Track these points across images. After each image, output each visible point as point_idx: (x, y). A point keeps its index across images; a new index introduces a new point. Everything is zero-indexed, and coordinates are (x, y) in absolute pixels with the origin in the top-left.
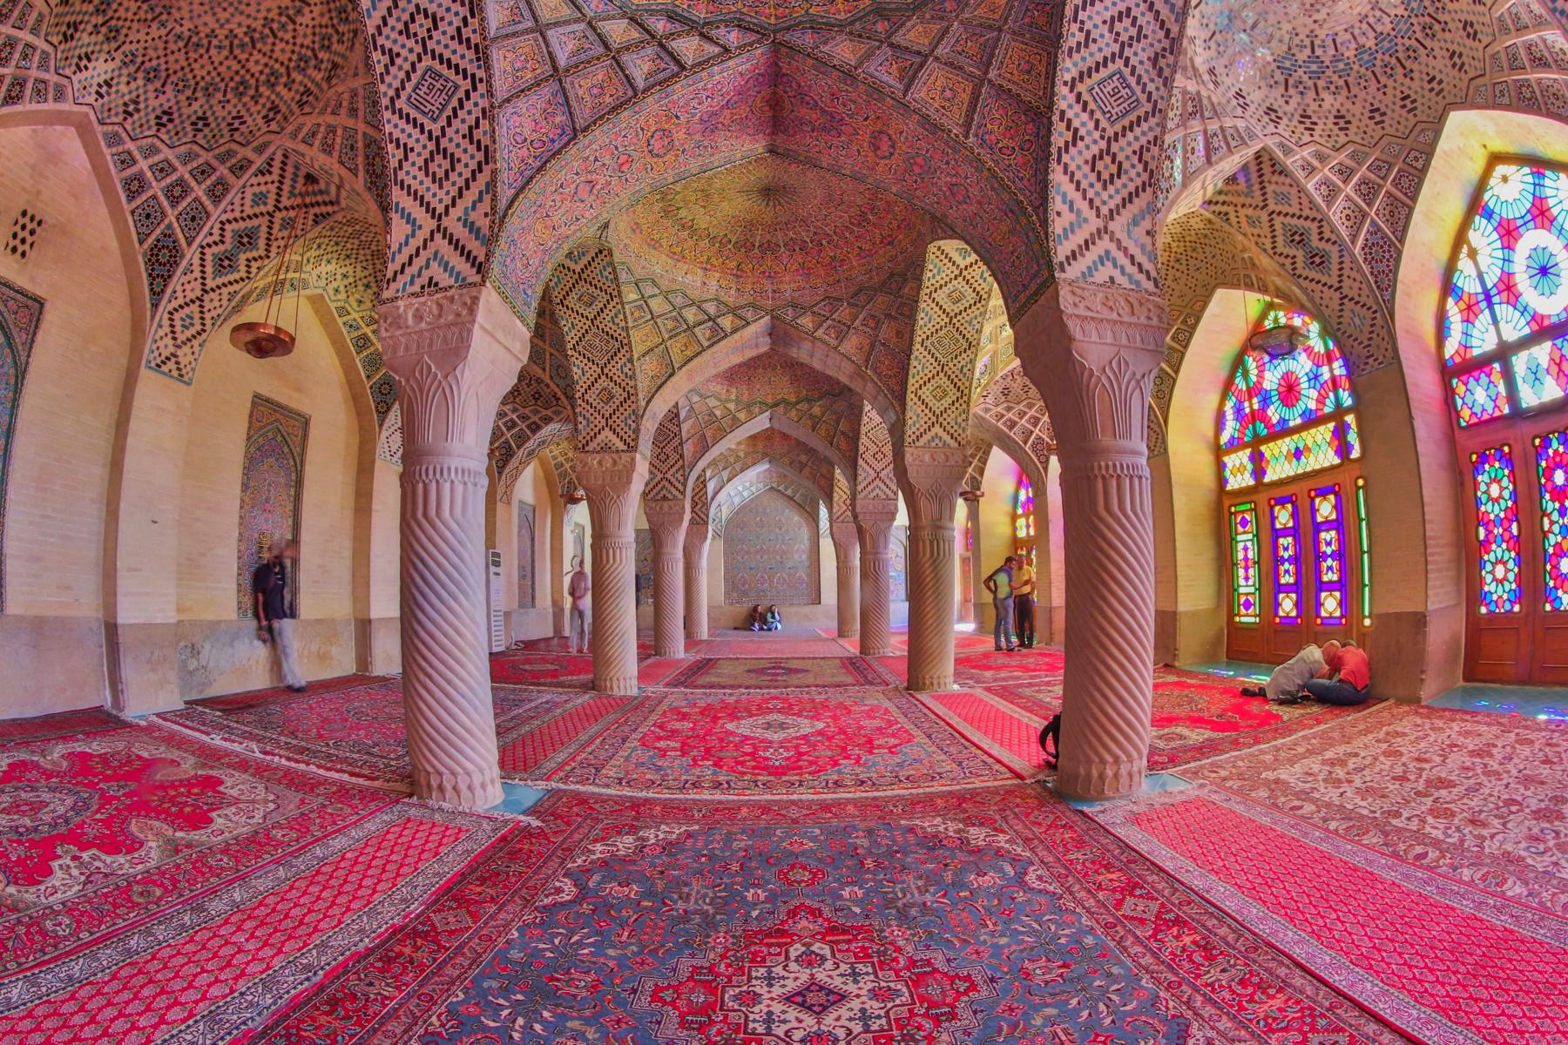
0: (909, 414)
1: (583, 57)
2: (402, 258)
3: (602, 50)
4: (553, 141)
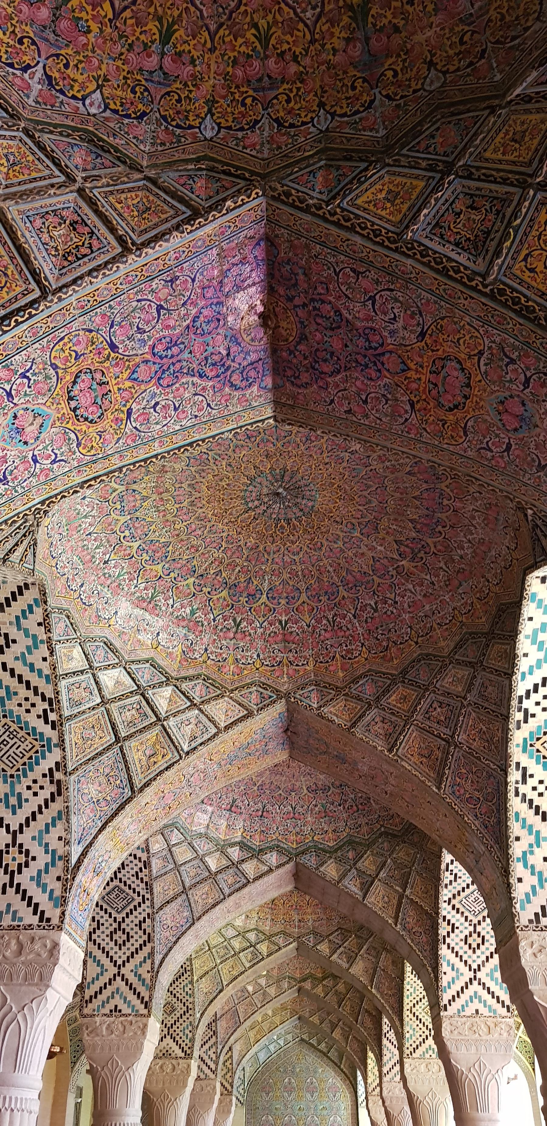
0: (406, 1028)
1: (198, 879)
2: (95, 987)
3: (207, 874)
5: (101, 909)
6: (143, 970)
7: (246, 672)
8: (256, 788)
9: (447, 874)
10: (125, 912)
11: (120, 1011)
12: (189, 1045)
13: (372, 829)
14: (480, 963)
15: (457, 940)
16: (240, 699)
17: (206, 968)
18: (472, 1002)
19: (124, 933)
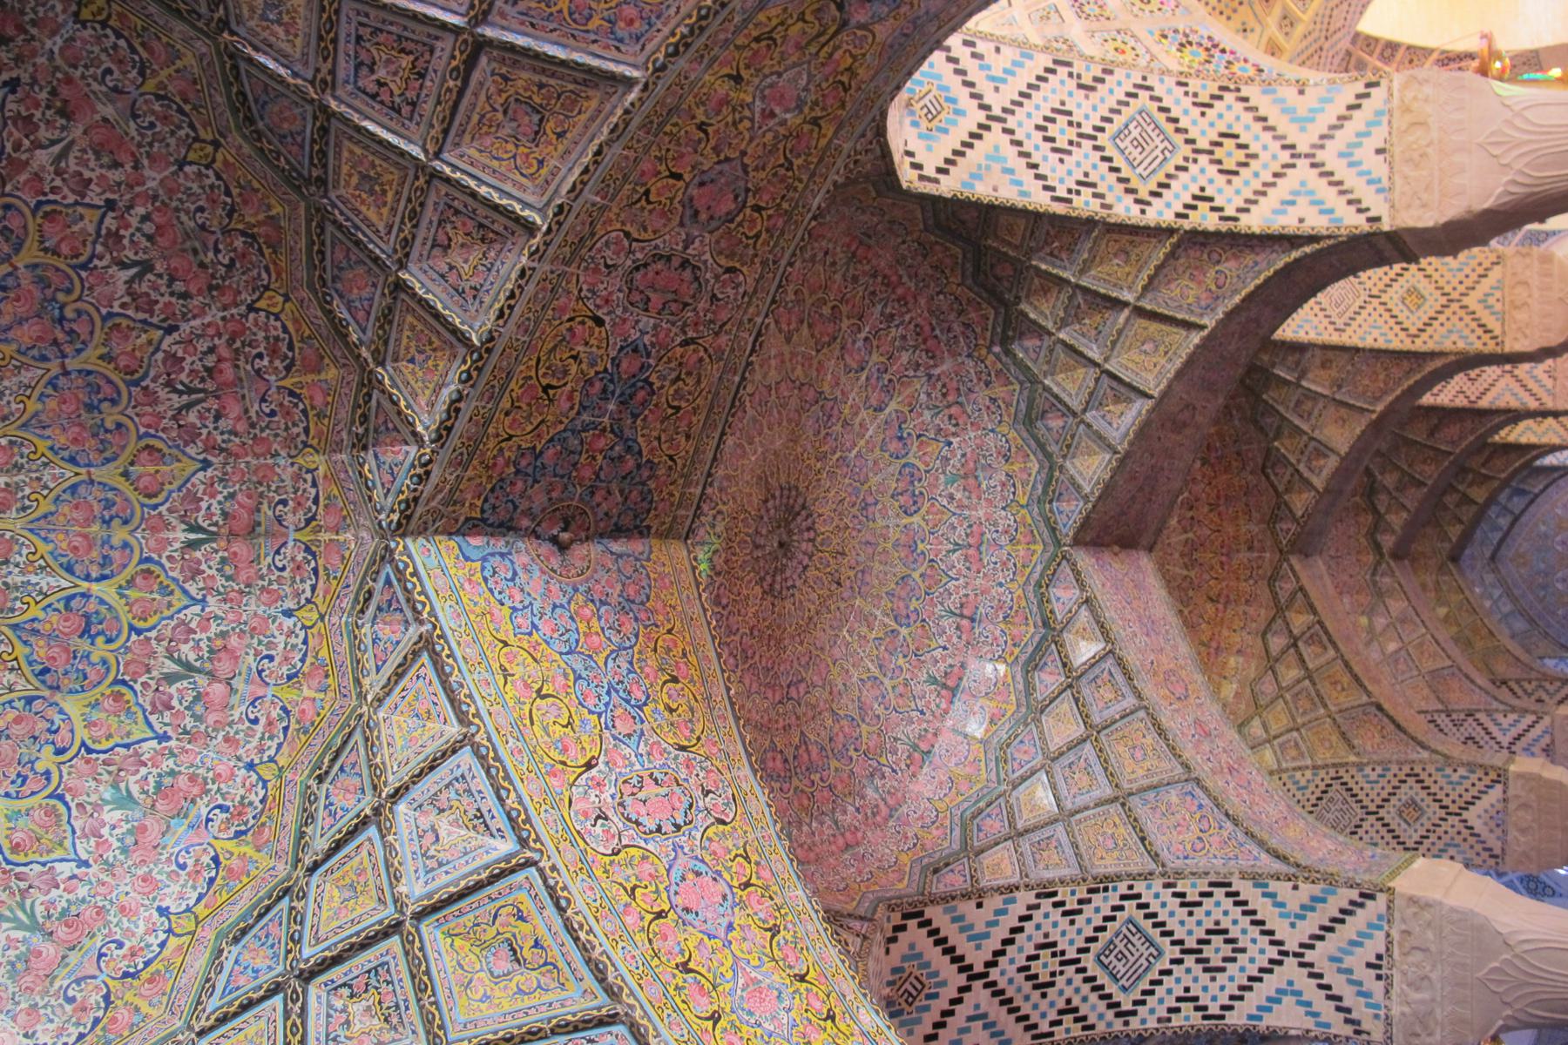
0: (1447, 346)
1: (1098, 769)
2: (1327, 1009)
3: (1088, 746)
4: (1200, 807)
6: (1294, 898)
7: (324, 653)
8: (904, 631)
10: (1159, 940)
11: (1379, 957)
12: (1480, 773)
13: (999, 373)
14: (1278, 144)
16: (388, 670)
17: (1334, 738)
19: (1208, 942)
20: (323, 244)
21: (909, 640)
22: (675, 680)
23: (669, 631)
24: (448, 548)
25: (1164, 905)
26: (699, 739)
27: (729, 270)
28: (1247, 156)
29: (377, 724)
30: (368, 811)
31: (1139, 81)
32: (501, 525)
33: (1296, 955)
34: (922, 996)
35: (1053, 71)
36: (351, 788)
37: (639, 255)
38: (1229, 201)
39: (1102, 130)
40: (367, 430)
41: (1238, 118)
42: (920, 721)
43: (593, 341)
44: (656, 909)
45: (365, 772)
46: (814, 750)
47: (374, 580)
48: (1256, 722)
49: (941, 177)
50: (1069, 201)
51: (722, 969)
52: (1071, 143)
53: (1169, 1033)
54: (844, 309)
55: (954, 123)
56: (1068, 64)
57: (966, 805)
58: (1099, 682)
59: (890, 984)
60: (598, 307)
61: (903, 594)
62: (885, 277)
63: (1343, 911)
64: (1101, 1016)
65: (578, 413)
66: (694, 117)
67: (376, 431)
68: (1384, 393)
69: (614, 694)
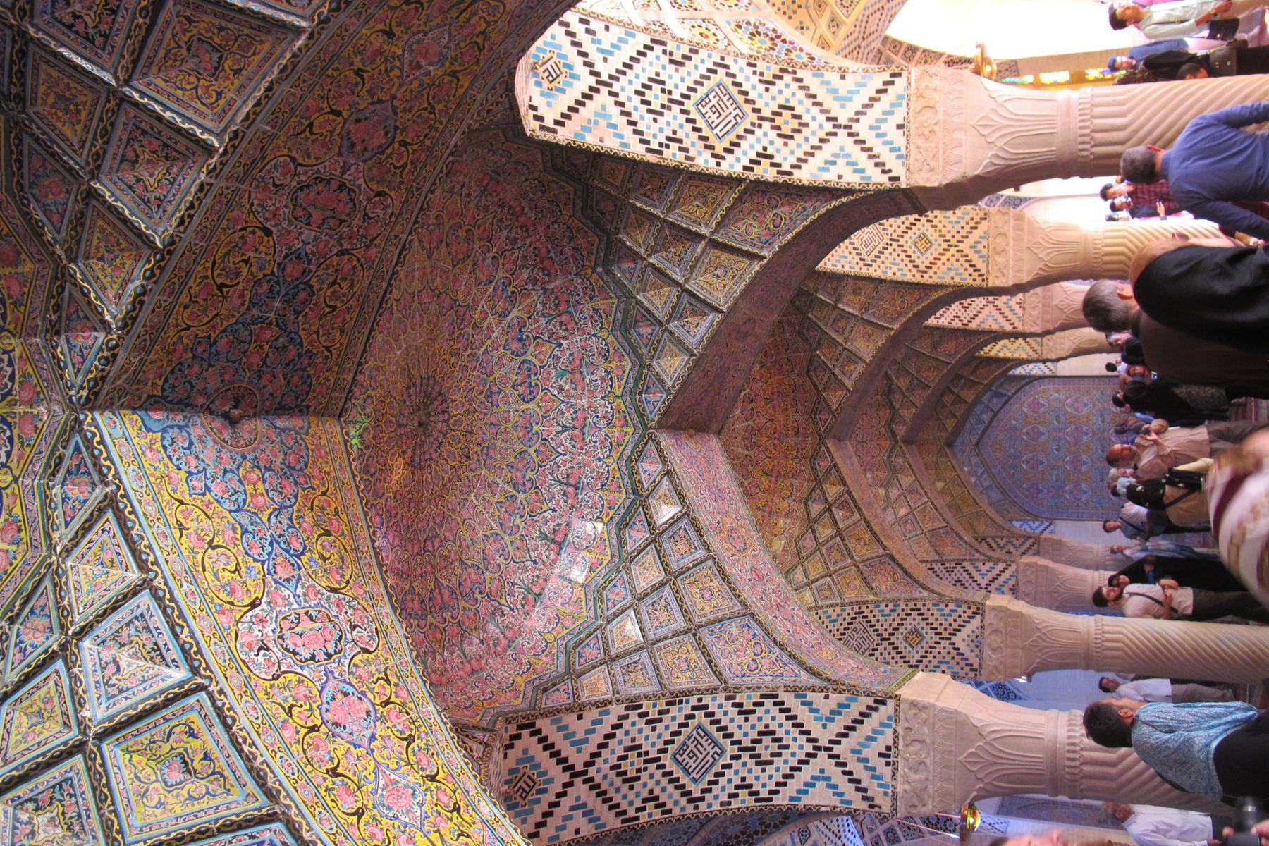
0: (947, 280)
1: (675, 606)
2: (849, 790)
3: (667, 588)
4: (755, 635)
5: (716, 782)
6: (825, 705)
7: (17, 511)
8: (521, 496)
9: (667, 153)
10: (722, 741)
11: (888, 748)
12: (964, 607)
13: (601, 289)
14: (823, 117)
15: (785, 151)
17: (858, 582)
18: (884, 135)
19: (759, 741)
20: (21, 153)
21: (525, 503)
22: (328, 534)
23: (324, 494)
24: (132, 421)
25: (726, 713)
26: (348, 582)
27: (379, 194)
28: (800, 124)
29: (65, 572)
30: (55, 647)
31: (719, 61)
32: (180, 402)
33: (827, 749)
34: (534, 791)
35: (651, 49)
36: (41, 628)
37: (303, 178)
38: (785, 159)
39: (688, 97)
40: (59, 317)
41: (794, 94)
42: (533, 569)
43: (261, 249)
44: (310, 724)
45: (54, 614)
46: (446, 594)
47: (65, 448)
48: (799, 570)
49: (558, 128)
50: (660, 153)
51: (366, 773)
52: (663, 106)
53: (729, 813)
54: (477, 232)
55: (571, 85)
56: (663, 43)
57: (570, 636)
58: (677, 537)
59: (507, 782)
60: (267, 219)
61: (520, 466)
62: (510, 208)
63: (862, 714)
64: (676, 803)
65: (248, 309)
66: (352, 64)
67: (68, 318)
68: (900, 315)
69: (275, 545)
